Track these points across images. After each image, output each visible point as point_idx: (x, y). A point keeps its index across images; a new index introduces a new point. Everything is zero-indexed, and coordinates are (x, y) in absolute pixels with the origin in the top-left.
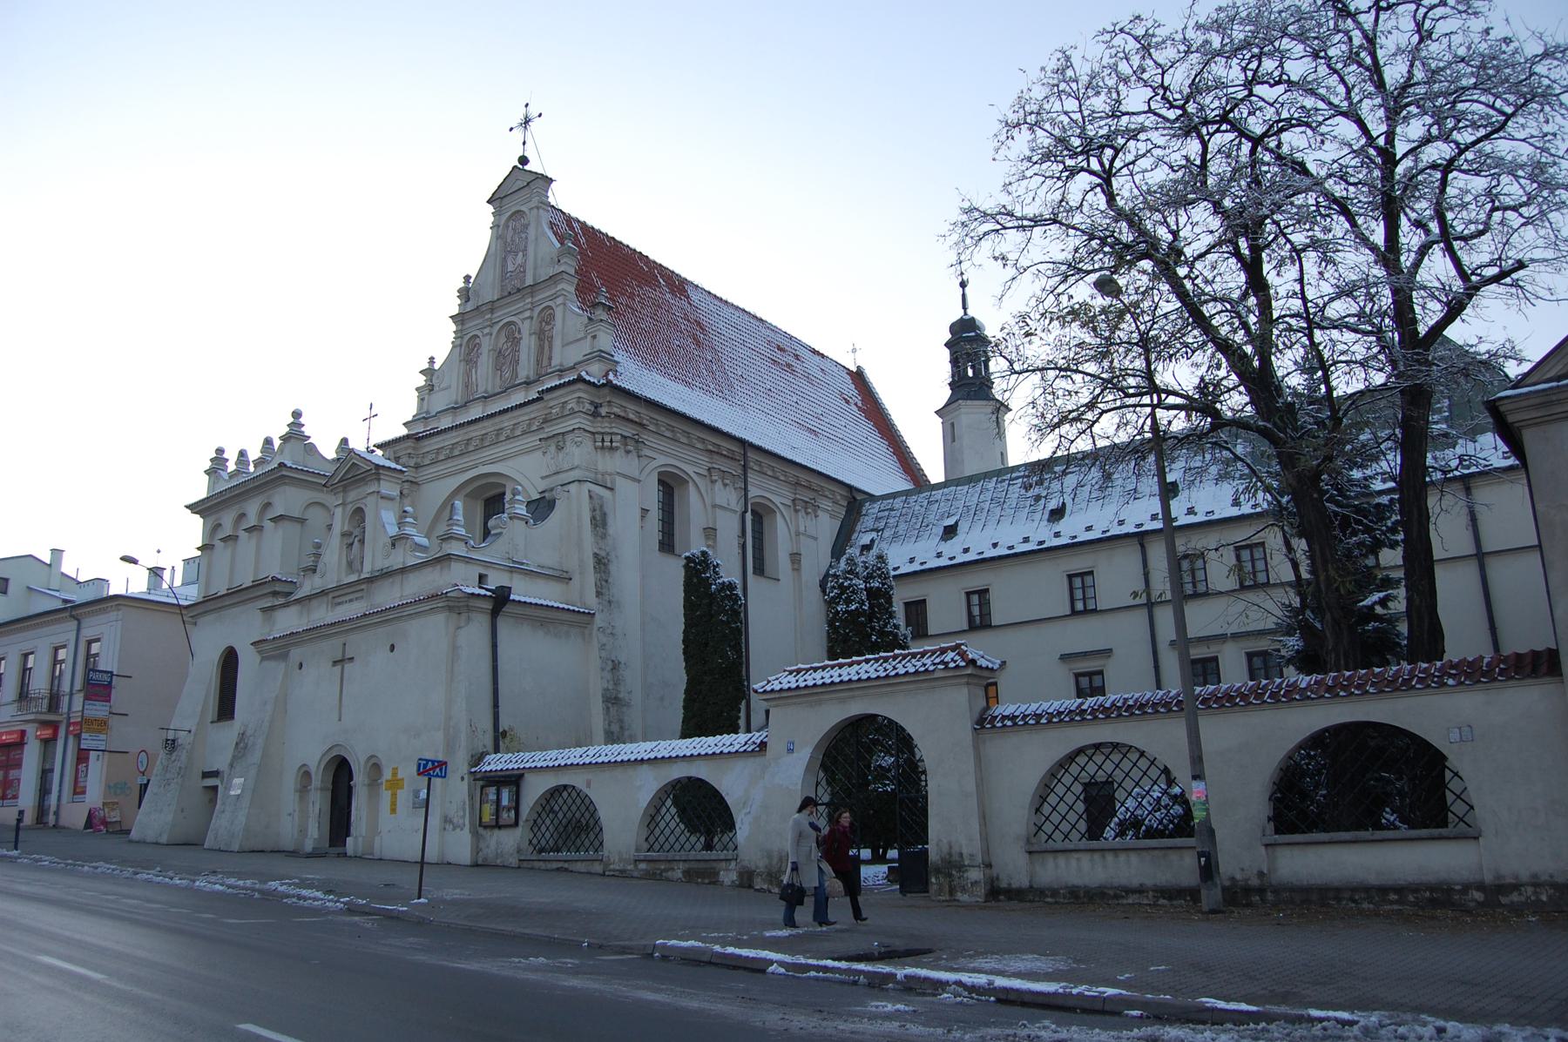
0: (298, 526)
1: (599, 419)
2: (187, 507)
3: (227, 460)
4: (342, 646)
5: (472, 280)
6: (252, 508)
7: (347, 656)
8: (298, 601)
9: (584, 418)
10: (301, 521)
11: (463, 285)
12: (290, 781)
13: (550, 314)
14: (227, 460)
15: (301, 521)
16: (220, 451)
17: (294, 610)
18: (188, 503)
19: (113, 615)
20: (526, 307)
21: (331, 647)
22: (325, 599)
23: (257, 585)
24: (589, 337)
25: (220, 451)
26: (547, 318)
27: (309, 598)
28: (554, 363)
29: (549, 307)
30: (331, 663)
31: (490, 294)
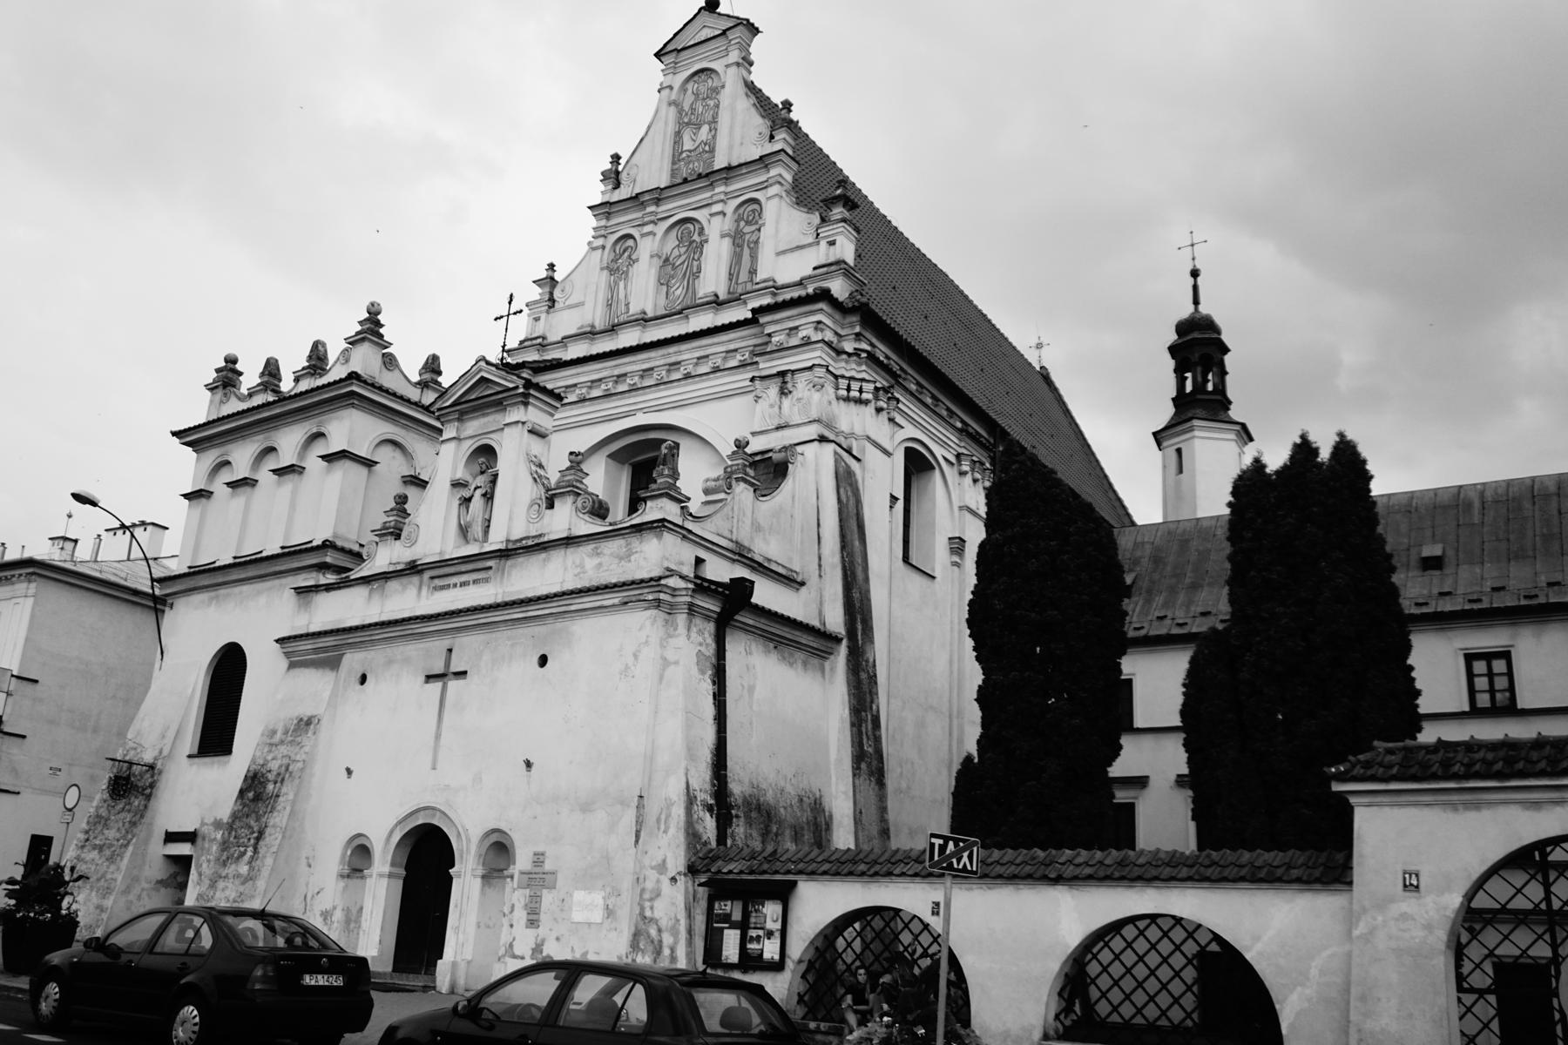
0: (363, 471)
1: (844, 356)
2: (174, 434)
3: (241, 374)
4: (444, 653)
5: (623, 161)
6: (288, 441)
7: (455, 668)
8: (366, 580)
9: (828, 355)
10: (369, 464)
11: (609, 166)
12: (331, 858)
13: (753, 211)
14: (241, 374)
15: (369, 464)
16: (231, 361)
17: (357, 594)
18: (174, 430)
19: (21, 587)
20: (715, 198)
21: (428, 653)
22: (415, 579)
23: (289, 553)
24: (823, 243)
25: (231, 361)
26: (751, 211)
27: (385, 576)
28: (760, 276)
29: (755, 201)
30: (423, 678)
31: (652, 173)
